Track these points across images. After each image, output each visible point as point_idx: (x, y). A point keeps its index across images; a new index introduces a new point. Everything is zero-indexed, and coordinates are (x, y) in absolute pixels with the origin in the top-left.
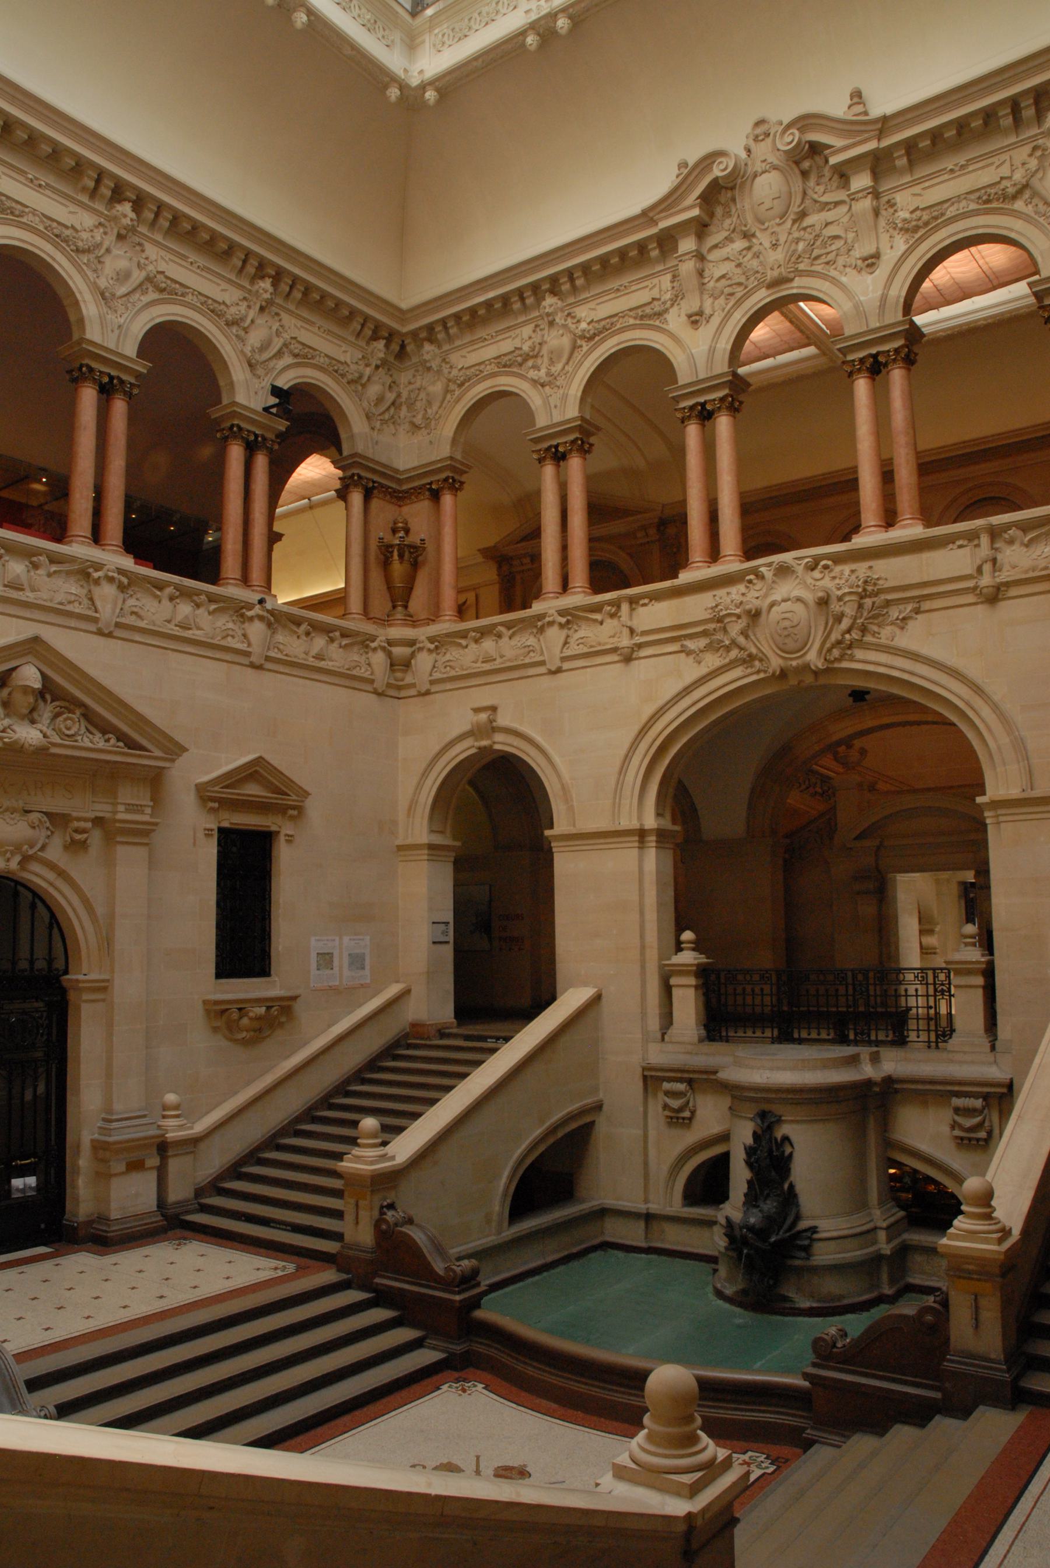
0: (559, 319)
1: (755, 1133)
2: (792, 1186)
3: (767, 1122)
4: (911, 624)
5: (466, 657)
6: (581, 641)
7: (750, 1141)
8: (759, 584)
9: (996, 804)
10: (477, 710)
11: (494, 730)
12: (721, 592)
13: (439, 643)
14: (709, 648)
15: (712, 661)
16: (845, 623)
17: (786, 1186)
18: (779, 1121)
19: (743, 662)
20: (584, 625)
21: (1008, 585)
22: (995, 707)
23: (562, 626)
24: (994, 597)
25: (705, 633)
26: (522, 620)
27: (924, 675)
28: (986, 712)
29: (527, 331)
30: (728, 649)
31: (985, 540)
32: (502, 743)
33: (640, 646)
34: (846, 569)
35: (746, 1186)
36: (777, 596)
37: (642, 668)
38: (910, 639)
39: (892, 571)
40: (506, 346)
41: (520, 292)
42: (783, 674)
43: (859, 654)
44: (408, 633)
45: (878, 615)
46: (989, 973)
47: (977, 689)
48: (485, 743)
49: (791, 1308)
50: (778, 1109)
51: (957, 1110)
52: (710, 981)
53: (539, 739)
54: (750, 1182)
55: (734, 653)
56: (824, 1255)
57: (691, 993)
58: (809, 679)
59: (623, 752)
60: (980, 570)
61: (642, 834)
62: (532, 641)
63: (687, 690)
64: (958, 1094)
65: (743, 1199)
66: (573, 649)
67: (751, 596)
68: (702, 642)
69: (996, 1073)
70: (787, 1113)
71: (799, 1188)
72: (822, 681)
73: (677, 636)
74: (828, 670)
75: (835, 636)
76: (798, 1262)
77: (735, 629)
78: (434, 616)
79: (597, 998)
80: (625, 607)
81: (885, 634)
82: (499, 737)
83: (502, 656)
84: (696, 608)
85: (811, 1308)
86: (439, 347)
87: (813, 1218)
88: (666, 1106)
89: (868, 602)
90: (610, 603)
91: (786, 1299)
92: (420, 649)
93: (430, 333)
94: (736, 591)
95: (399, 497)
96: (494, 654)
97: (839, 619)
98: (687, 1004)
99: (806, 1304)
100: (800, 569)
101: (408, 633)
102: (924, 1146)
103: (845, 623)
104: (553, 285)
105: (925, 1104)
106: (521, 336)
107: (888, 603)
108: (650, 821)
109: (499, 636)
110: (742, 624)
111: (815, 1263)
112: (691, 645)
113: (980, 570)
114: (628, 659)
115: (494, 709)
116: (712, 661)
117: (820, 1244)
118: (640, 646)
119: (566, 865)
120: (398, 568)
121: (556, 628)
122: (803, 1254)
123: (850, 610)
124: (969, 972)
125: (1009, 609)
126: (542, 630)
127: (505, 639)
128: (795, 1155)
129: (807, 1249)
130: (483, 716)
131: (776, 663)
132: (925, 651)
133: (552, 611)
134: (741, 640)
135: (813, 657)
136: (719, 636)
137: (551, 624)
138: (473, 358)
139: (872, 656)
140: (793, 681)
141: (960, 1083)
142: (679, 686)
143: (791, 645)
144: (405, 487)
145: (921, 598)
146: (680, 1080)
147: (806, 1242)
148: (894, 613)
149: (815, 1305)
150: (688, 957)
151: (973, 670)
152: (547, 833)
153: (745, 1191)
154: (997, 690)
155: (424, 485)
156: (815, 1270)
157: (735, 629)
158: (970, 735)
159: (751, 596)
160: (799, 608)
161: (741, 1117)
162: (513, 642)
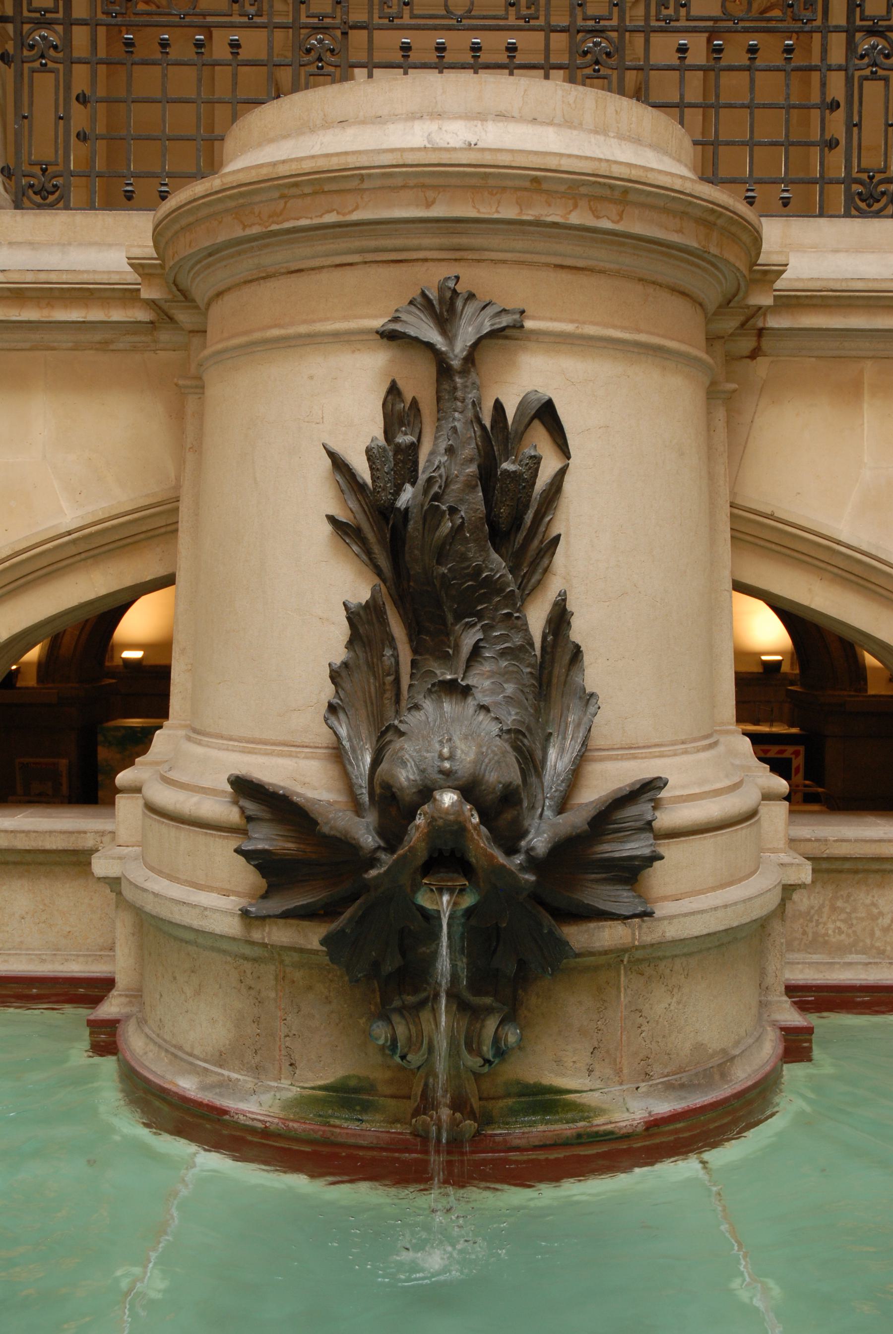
1: (394, 391)
2: (560, 618)
3: (443, 354)
17: (536, 617)
35: (341, 631)
49: (580, 1139)
50: (503, 285)
56: (694, 891)
65: (327, 691)
70: (547, 302)
71: (580, 630)
76: (608, 935)
85: (654, 1124)
87: (630, 750)
91: (544, 1101)
99: (629, 1108)
105: (850, 392)
111: (672, 931)
117: (672, 851)
122: (619, 898)
128: (569, 485)
129: (631, 872)
147: (636, 847)
149: (663, 1107)
153: (339, 654)
156: (648, 961)
161: (313, 340)
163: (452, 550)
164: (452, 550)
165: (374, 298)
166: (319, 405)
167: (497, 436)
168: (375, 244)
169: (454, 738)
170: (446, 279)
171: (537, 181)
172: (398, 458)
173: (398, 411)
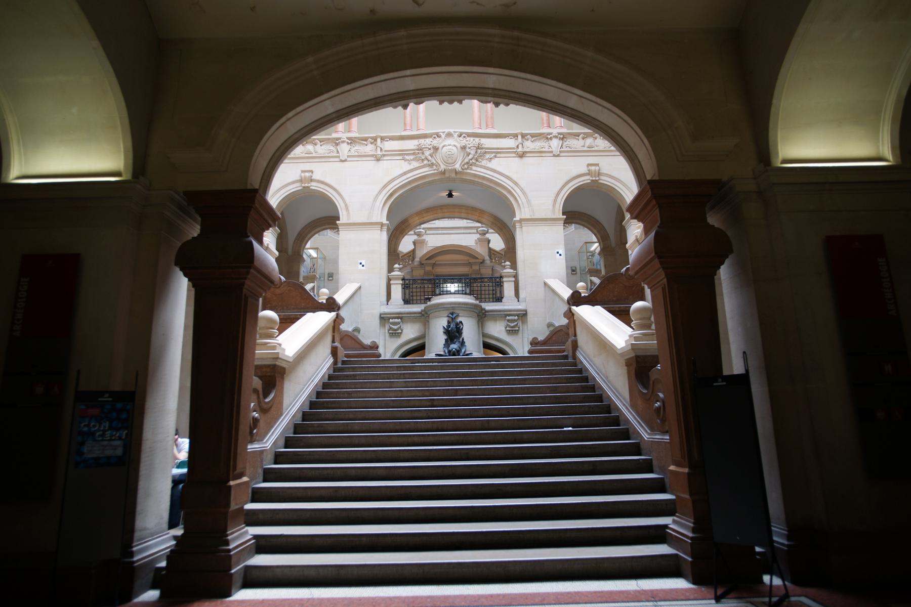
3: (452, 317)
4: (493, 161)
6: (357, 151)
7: (445, 324)
8: (438, 139)
9: (521, 221)
10: (303, 172)
11: (312, 180)
12: (422, 141)
14: (413, 159)
15: (416, 164)
16: (471, 156)
18: (458, 316)
19: (429, 165)
21: (527, 152)
22: (522, 190)
23: (348, 143)
24: (522, 155)
25: (414, 154)
26: (329, 139)
27: (497, 178)
28: (518, 191)
30: (423, 160)
31: (520, 137)
32: (314, 186)
33: (384, 155)
34: (472, 139)
36: (446, 143)
37: (385, 164)
38: (494, 164)
39: (487, 143)
42: (444, 173)
43: (474, 168)
45: (482, 156)
46: (516, 276)
47: (516, 184)
50: (457, 312)
51: (508, 321)
52: (407, 285)
53: (334, 185)
54: (446, 340)
55: (426, 162)
57: (400, 286)
58: (453, 175)
59: (376, 193)
60: (518, 147)
61: (382, 225)
62: (332, 148)
63: (405, 173)
64: (509, 315)
66: (353, 153)
67: (436, 142)
68: (412, 157)
72: (458, 176)
73: (402, 154)
74: (460, 173)
75: (466, 160)
77: (427, 153)
79: (360, 287)
80: (379, 140)
81: (484, 163)
82: (313, 184)
84: (411, 145)
88: (391, 329)
89: (479, 151)
90: (371, 138)
94: (428, 141)
97: (469, 154)
98: (397, 291)
100: (456, 136)
102: (496, 335)
103: (471, 156)
105: (496, 320)
107: (486, 153)
108: (385, 221)
110: (432, 151)
112: (407, 157)
113: (518, 147)
114: (378, 160)
115: (312, 172)
116: (416, 164)
118: (384, 155)
123: (473, 152)
124: (509, 276)
125: (527, 160)
126: (337, 144)
127: (318, 146)
130: (307, 174)
131: (443, 167)
132: (498, 169)
134: (429, 158)
135: (458, 167)
136: (420, 155)
137: (343, 142)
139: (479, 169)
140: (447, 175)
141: (510, 311)
142: (402, 172)
143: (450, 161)
145: (497, 152)
146: (398, 318)
148: (488, 156)
151: (514, 177)
154: (522, 184)
157: (427, 153)
158: (511, 199)
159: (436, 142)
160: (454, 148)
162: (323, 147)
163: (453, 334)
164: (453, 334)
165: (446, 313)
166: (440, 324)
167: (457, 324)
168: (447, 309)
169: (454, 346)
170: (452, 312)
171: (459, 303)
172: (449, 326)
173: (449, 322)
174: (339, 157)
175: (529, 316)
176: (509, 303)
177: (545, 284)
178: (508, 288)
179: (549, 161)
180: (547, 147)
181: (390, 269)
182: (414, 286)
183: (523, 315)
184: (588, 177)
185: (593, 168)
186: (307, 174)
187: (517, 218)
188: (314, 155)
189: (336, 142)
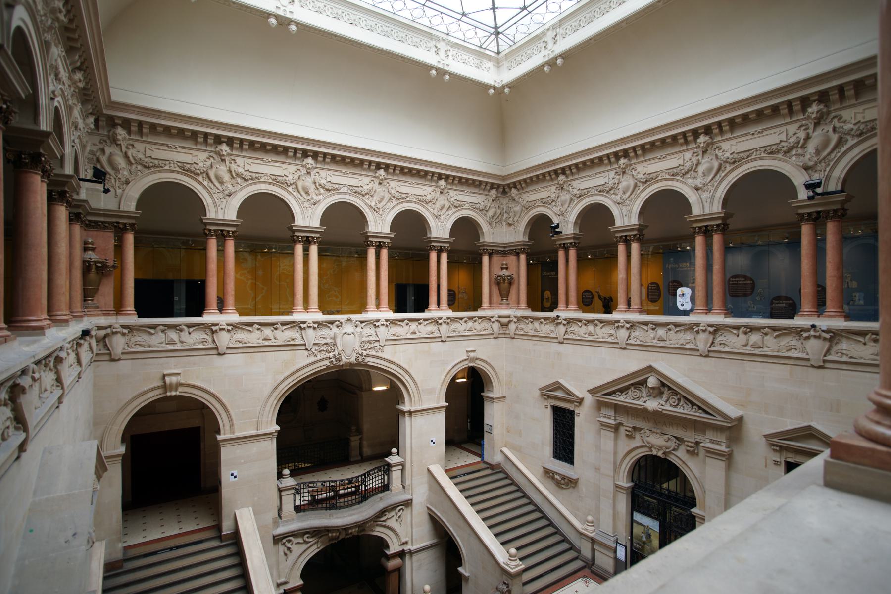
0: (227, 159)
5: (157, 340)
13: (131, 328)
20: (239, 331)
29: (203, 156)
40: (184, 157)
41: (206, 135)
44: (103, 321)
46: (403, 465)
48: (174, 393)
69: (409, 497)
78: (119, 309)
82: (180, 389)
83: (182, 342)
86: (129, 133)
92: (116, 333)
93: (126, 124)
95: (90, 226)
96: (177, 340)
101: (103, 321)
104: (230, 141)
106: (200, 158)
109: (181, 330)
115: (179, 374)
119: (226, 454)
120: (93, 274)
121: (224, 333)
126: (213, 332)
133: (223, 323)
138: (160, 153)
144: (90, 218)
150: (289, 482)
152: (219, 437)
155: (112, 223)
174: (217, 349)
175: (414, 502)
176: (396, 495)
177: (428, 470)
178: (396, 474)
179: (436, 346)
180: (437, 330)
181: (280, 476)
182: (306, 490)
183: (408, 503)
184: (466, 362)
185: (472, 355)
186: (174, 379)
187: (406, 407)
188: (179, 346)
189: (211, 329)
